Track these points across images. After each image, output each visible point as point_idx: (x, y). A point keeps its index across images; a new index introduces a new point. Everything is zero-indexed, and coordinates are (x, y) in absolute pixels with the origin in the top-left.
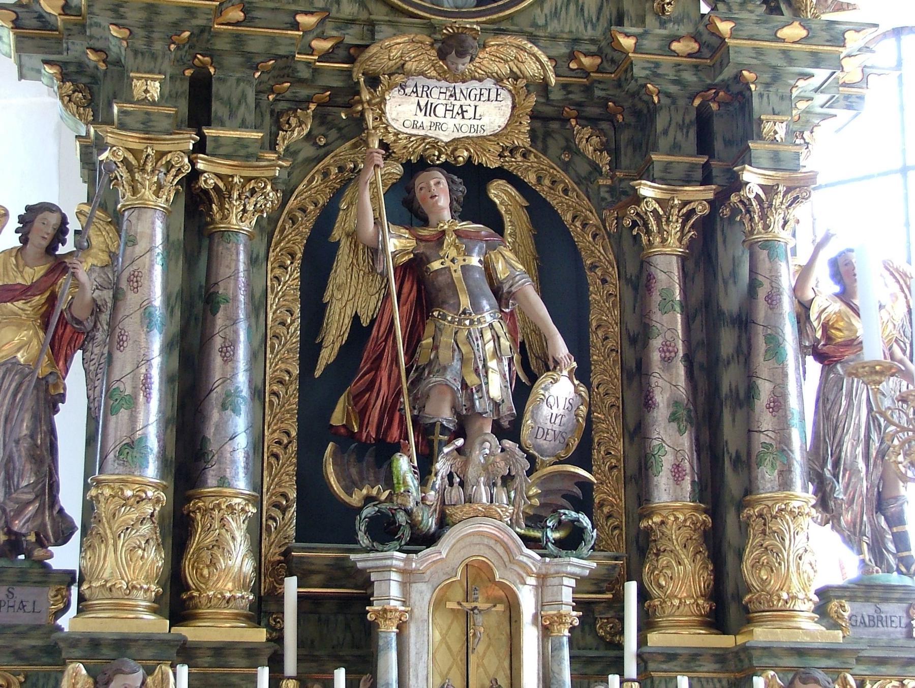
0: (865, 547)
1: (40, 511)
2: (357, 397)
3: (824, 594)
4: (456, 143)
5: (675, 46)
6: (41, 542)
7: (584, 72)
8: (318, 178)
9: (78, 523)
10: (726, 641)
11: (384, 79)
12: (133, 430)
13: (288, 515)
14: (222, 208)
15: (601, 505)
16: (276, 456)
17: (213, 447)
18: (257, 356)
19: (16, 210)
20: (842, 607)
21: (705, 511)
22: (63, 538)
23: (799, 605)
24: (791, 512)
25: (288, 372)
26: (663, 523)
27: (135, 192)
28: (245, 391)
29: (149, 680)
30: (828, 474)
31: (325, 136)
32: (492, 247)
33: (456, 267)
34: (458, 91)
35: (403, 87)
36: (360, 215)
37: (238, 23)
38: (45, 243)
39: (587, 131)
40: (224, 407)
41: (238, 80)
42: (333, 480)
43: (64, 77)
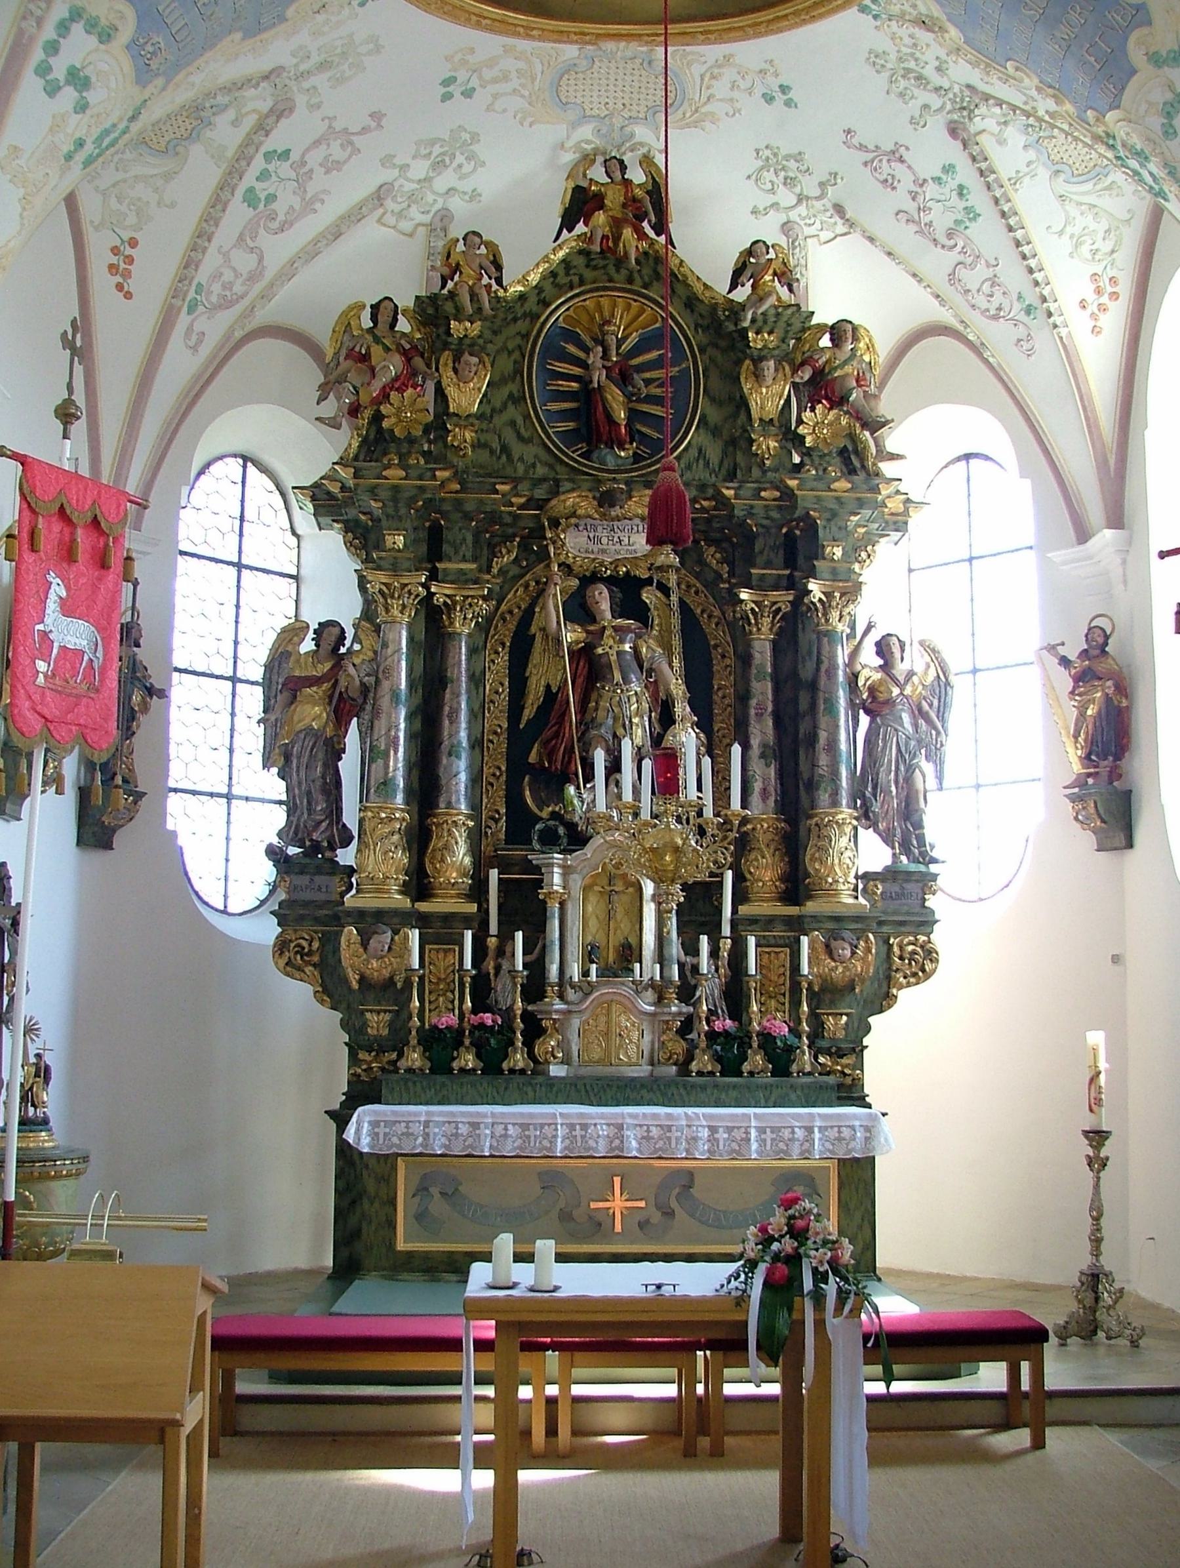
0: (897, 845)
1: (330, 825)
2: (545, 744)
3: (867, 877)
4: (616, 563)
5: (763, 494)
6: (332, 848)
7: (703, 510)
8: (521, 590)
9: (355, 834)
10: (793, 910)
11: (563, 521)
12: (387, 773)
13: (500, 825)
14: (449, 617)
16: (492, 785)
17: (443, 782)
18: (476, 715)
19: (314, 626)
20: (876, 886)
21: (785, 821)
22: (346, 841)
23: (841, 887)
24: (837, 823)
25: (500, 726)
26: (754, 829)
27: (387, 611)
28: (465, 744)
29: (396, 938)
30: (868, 794)
31: (527, 560)
32: (639, 636)
33: (613, 652)
35: (577, 526)
36: (547, 615)
37: (457, 492)
38: (330, 648)
39: (712, 549)
40: (450, 754)
41: (460, 529)
42: (529, 800)
43: (347, 530)
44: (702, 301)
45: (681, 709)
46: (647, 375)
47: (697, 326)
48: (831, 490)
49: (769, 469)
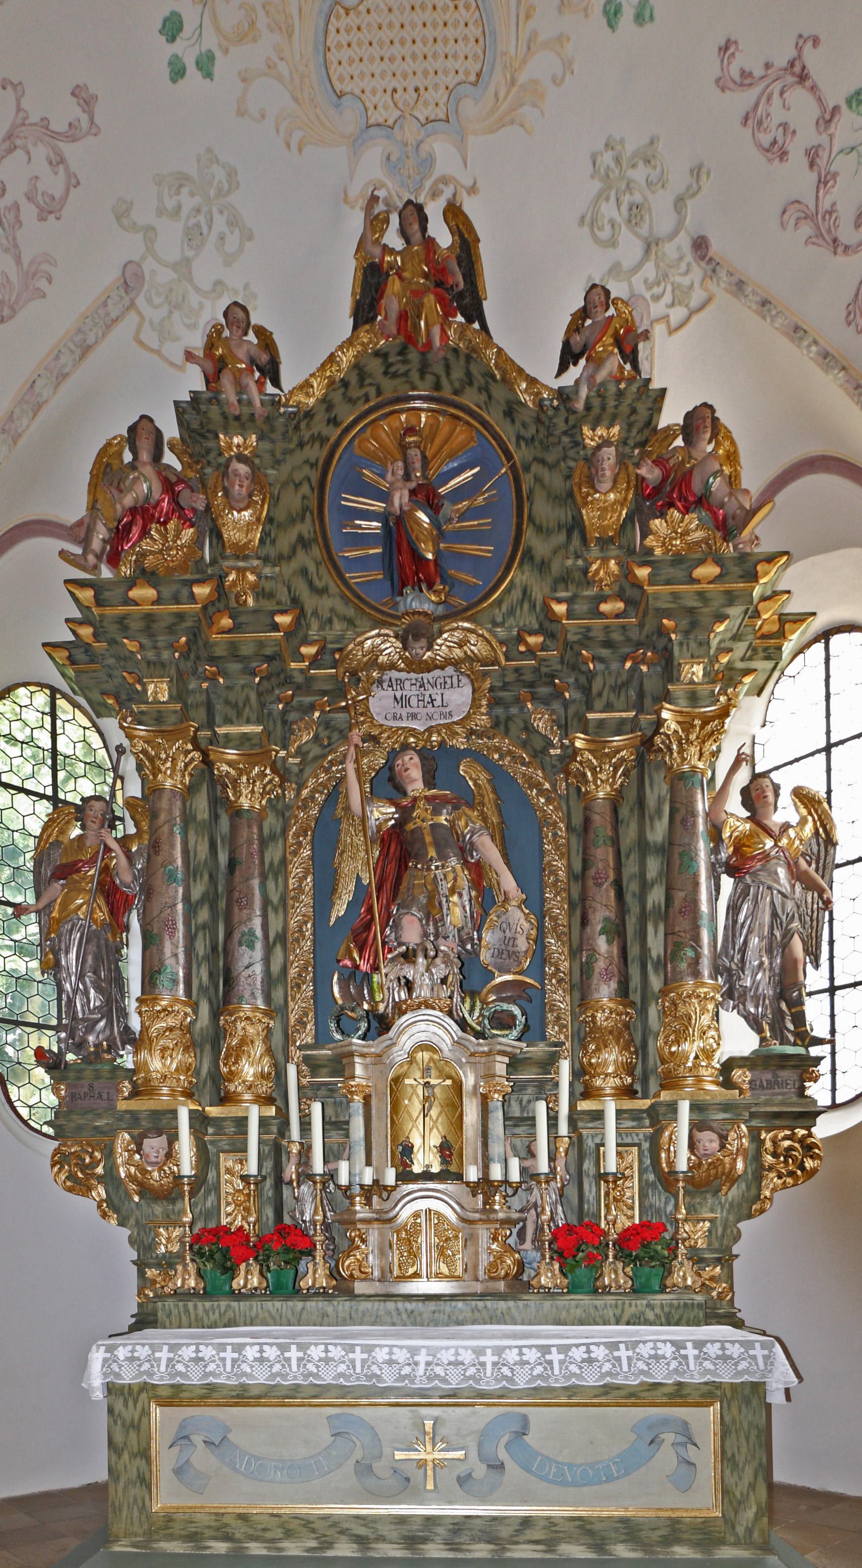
0: (766, 1027)
34: (425, 681)
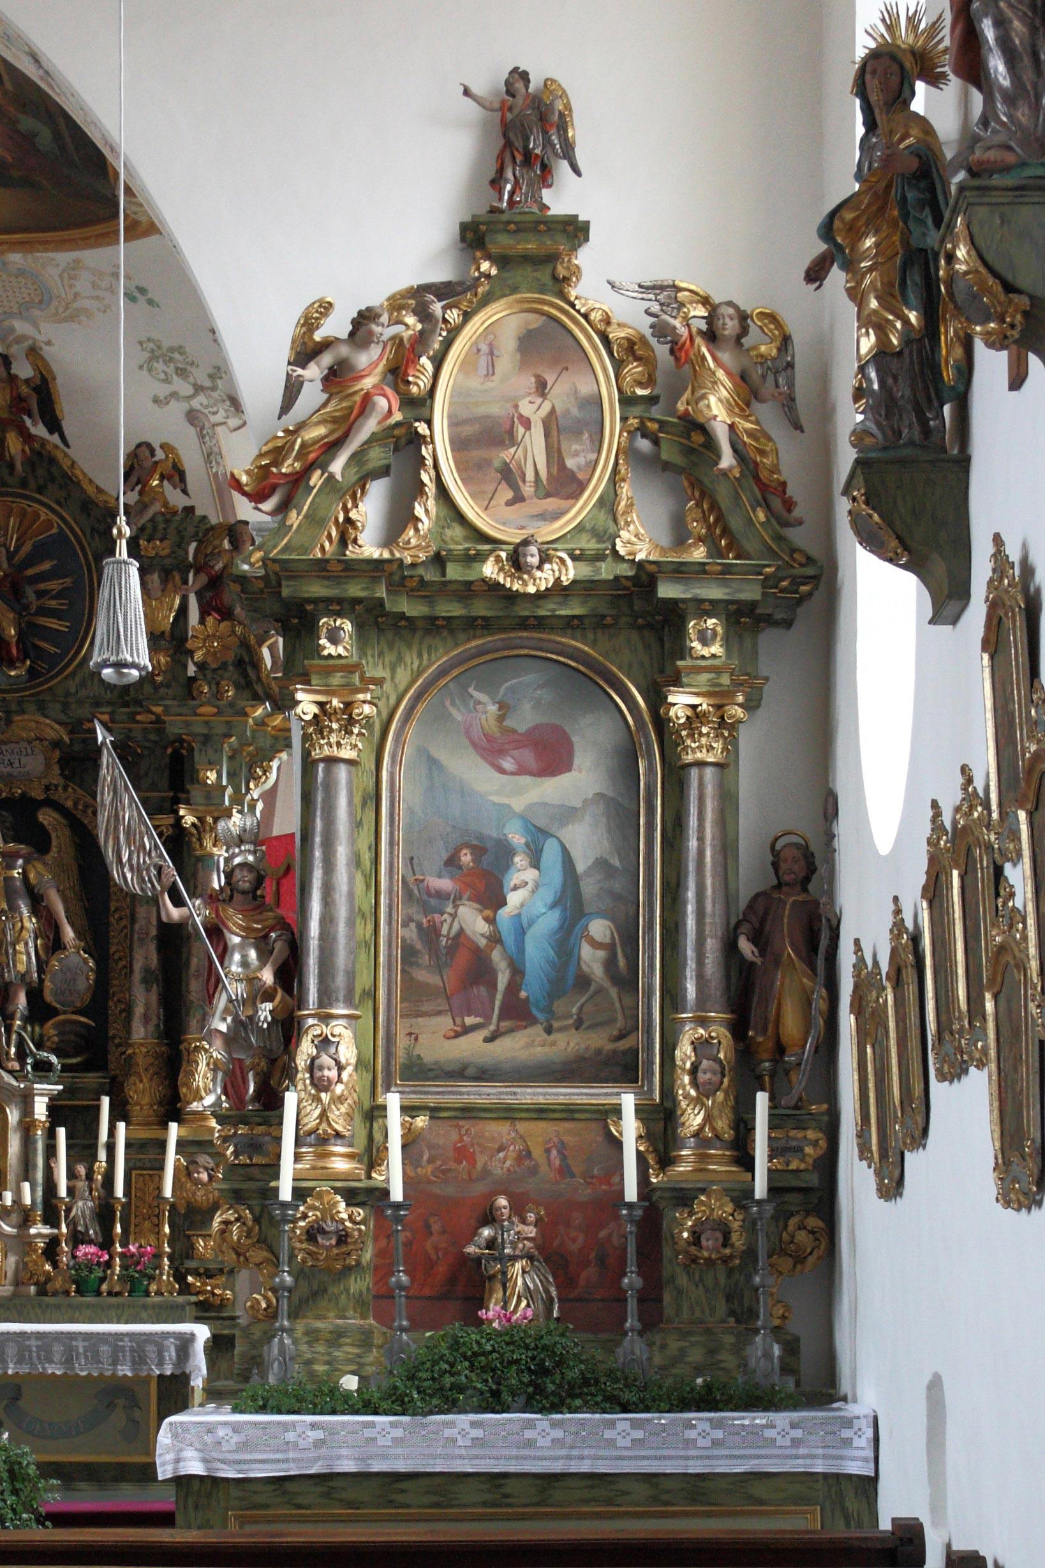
5: (138, 718)
15: (114, 1037)
44: (97, 505)
45: (69, 933)
46: (42, 586)
47: (93, 529)
48: (199, 715)
49: (161, 685)
